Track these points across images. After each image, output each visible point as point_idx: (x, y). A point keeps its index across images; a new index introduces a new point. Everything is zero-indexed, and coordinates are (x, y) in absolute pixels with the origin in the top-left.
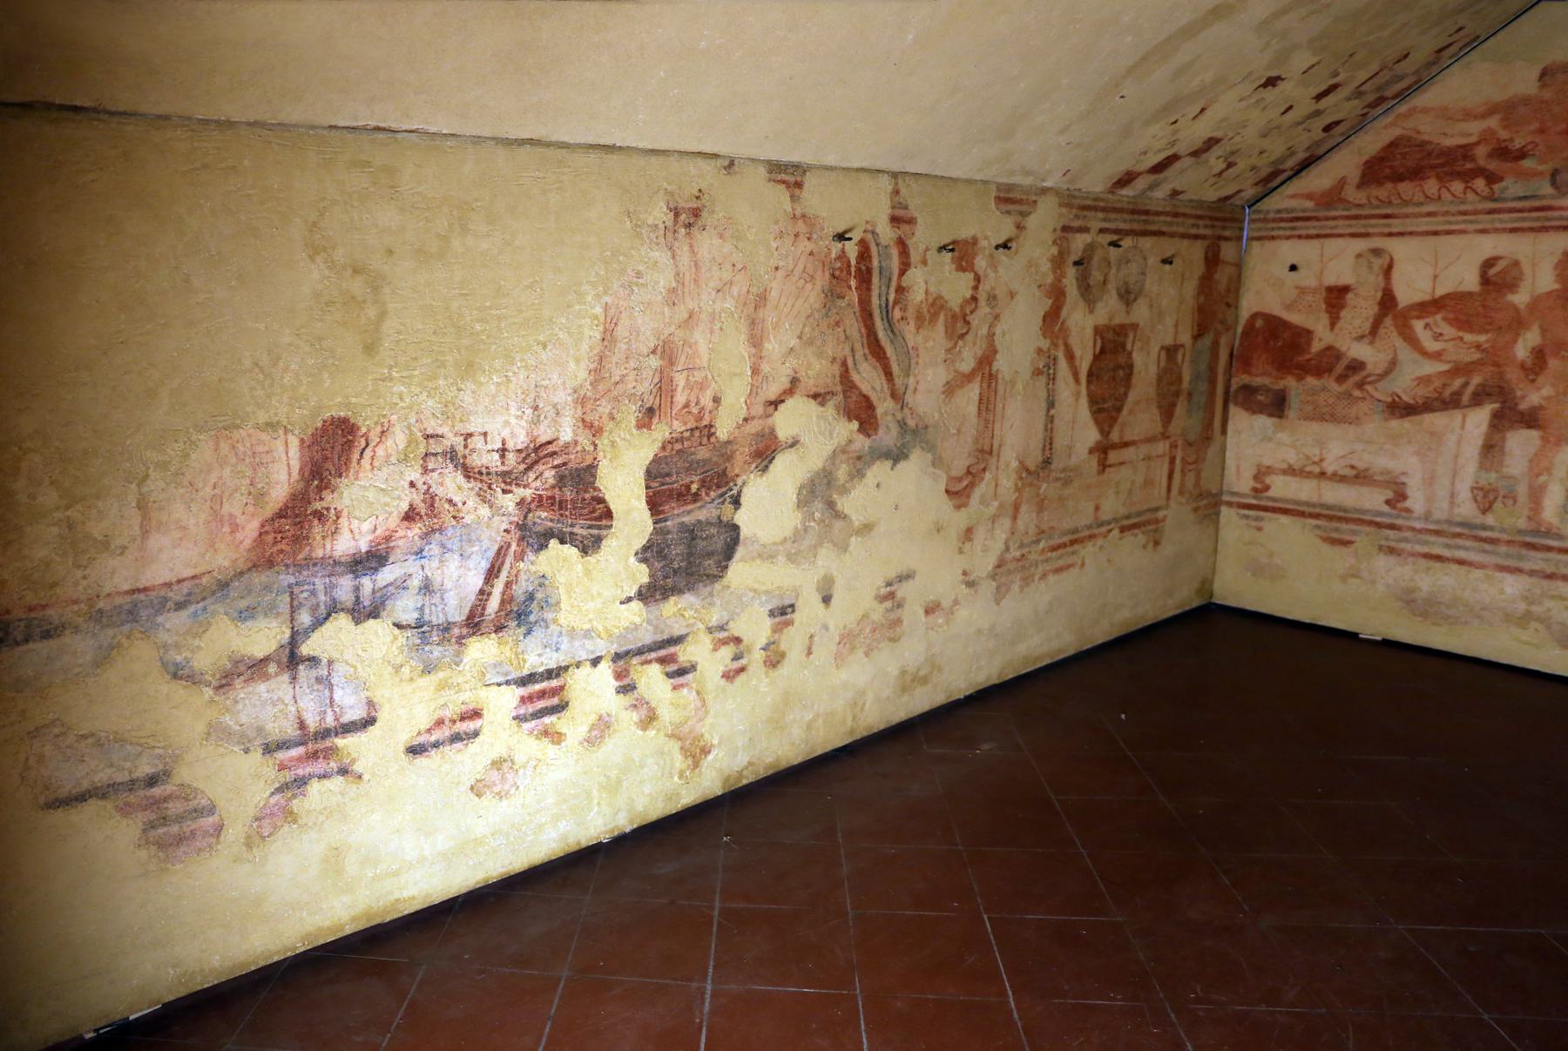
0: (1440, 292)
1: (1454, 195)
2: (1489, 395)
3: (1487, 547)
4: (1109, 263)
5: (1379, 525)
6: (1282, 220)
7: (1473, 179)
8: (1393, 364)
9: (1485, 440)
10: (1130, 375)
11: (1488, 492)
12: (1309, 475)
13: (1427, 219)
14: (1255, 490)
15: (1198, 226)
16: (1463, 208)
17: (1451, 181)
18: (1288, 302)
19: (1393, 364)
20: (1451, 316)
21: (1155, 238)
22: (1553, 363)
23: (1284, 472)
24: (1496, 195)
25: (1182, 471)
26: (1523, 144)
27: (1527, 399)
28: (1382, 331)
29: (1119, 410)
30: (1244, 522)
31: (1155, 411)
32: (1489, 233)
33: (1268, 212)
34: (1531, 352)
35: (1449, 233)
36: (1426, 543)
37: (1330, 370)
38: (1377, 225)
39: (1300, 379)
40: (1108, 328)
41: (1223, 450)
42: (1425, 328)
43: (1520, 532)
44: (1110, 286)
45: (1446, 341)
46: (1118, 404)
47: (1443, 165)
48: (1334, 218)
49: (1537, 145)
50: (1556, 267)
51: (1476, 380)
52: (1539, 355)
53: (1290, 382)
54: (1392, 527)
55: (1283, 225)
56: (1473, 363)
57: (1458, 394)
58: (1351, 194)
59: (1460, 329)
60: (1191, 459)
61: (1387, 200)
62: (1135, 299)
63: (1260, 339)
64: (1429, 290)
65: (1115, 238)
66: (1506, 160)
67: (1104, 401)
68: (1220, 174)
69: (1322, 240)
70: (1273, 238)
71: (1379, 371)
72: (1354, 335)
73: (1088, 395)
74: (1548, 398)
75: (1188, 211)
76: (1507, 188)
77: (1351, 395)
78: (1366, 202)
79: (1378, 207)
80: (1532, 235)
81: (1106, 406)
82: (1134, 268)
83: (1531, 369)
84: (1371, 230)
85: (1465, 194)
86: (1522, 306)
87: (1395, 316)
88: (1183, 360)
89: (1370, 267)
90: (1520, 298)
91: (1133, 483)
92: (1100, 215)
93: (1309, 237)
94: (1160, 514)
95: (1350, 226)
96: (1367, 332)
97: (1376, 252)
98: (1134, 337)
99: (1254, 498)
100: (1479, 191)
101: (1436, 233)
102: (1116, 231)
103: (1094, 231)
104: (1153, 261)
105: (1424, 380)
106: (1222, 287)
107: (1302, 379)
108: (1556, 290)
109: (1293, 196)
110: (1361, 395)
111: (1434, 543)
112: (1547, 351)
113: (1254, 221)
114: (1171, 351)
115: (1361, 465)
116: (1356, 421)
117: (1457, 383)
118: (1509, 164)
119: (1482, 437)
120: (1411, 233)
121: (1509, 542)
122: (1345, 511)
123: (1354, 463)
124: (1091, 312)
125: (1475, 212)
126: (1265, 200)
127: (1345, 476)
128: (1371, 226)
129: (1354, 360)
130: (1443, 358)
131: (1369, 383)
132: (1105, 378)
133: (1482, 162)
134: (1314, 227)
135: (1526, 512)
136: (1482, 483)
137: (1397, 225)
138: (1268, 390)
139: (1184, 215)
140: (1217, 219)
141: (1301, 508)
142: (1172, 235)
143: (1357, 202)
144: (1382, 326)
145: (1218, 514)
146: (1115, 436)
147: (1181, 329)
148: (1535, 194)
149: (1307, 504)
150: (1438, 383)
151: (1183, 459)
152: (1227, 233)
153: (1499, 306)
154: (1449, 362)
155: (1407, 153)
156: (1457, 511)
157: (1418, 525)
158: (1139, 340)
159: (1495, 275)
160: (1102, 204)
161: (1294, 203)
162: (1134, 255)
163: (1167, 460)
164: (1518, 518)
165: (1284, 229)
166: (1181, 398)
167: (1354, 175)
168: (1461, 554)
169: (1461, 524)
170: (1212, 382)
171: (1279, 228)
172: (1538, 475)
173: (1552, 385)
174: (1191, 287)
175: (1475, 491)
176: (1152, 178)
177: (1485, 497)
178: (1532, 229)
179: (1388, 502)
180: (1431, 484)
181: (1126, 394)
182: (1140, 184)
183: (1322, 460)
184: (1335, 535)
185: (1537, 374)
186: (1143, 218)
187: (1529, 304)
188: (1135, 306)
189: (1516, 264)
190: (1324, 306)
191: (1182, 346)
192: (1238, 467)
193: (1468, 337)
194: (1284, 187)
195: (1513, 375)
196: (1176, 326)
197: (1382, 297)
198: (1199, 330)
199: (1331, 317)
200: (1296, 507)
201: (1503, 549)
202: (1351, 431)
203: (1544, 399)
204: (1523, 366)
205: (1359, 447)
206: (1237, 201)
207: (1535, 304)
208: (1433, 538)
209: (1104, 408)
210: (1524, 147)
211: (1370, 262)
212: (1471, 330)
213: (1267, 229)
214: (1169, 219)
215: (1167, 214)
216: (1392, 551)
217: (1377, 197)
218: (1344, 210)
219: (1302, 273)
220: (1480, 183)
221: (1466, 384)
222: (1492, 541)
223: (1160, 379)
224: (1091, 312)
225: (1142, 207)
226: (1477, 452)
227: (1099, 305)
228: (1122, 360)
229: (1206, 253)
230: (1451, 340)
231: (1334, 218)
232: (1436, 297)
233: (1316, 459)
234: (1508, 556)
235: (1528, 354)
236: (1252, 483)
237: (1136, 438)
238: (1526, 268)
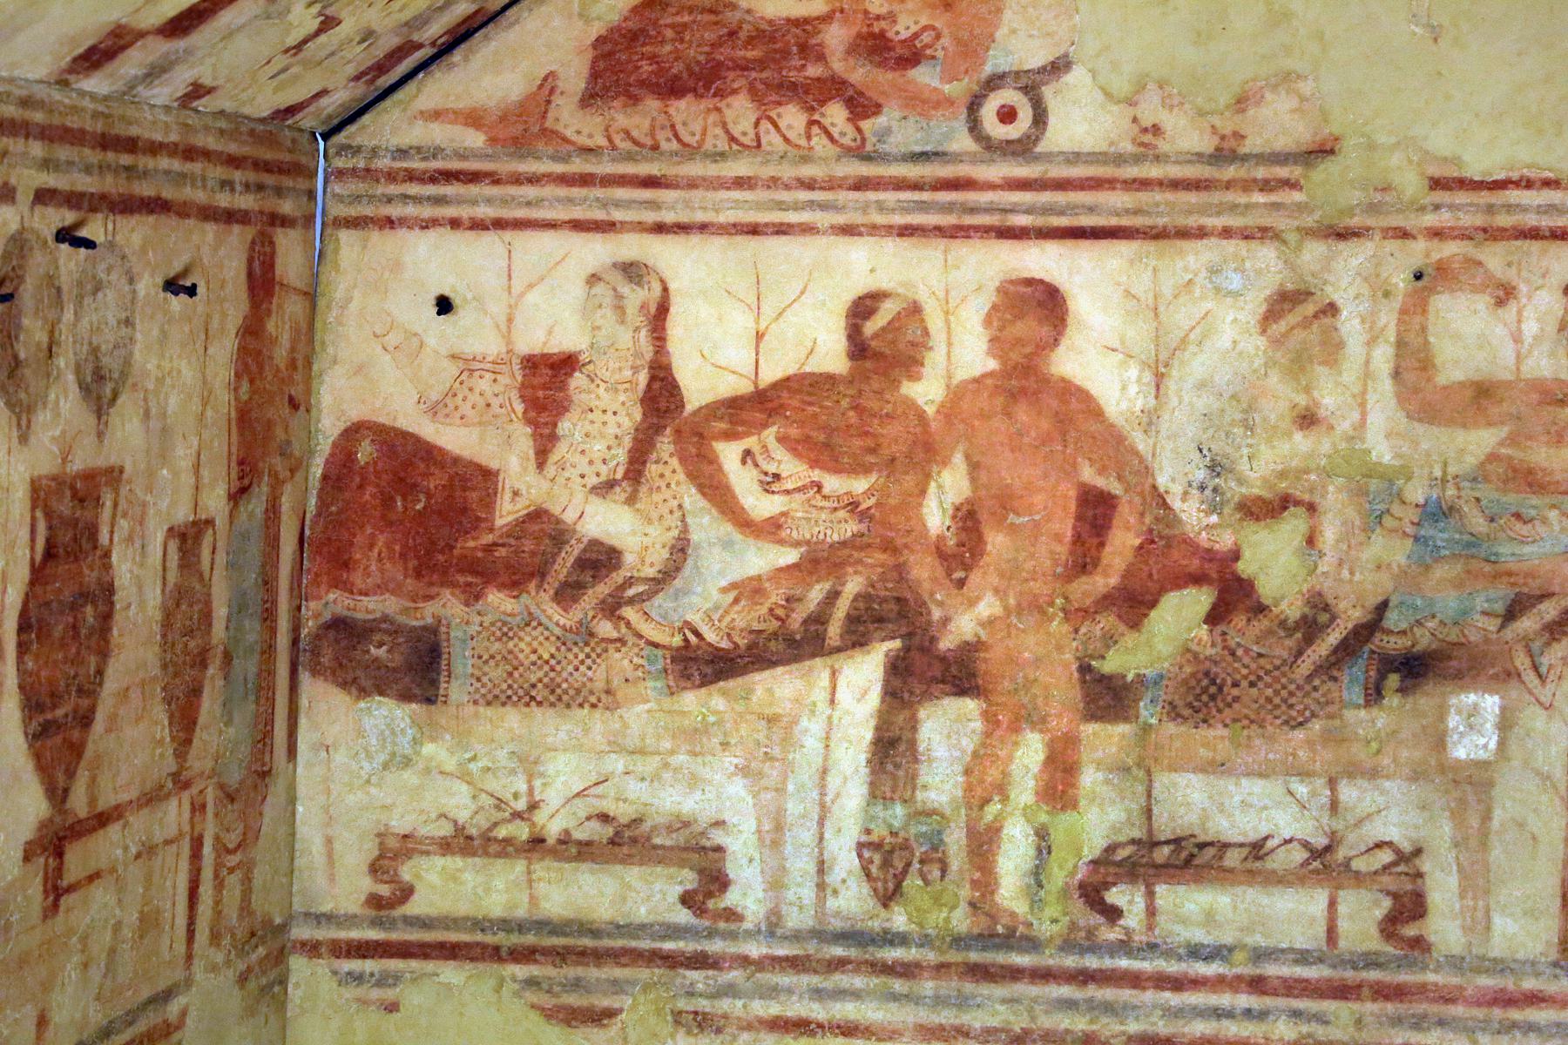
0: (771, 373)
1: (786, 140)
2: (880, 620)
3: (898, 985)
4: (59, 290)
5: (672, 961)
6: (411, 176)
7: (823, 103)
8: (681, 549)
9: (878, 729)
10: (107, 617)
11: (891, 852)
12: (506, 849)
13: (736, 194)
14: (375, 901)
15: (226, 184)
16: (807, 171)
17: (780, 104)
18: (434, 396)
19: (681, 549)
20: (794, 432)
21: (151, 219)
22: (996, 542)
23: (445, 847)
24: (869, 147)
25: (216, 876)
26: (914, 29)
27: (952, 626)
28: (652, 469)
29: (85, 720)
30: (351, 992)
31: (160, 713)
32: (860, 234)
33: (374, 152)
34: (954, 517)
35: (782, 230)
36: (772, 992)
37: (541, 573)
38: (627, 204)
39: (473, 596)
40: (60, 482)
41: (292, 800)
42: (744, 462)
43: (959, 941)
44: (61, 362)
45: (788, 492)
46: (85, 703)
47: (761, 64)
48: (533, 180)
49: (938, 37)
50: (987, 322)
51: (853, 586)
52: (968, 519)
53: (448, 607)
54: (701, 961)
55: (414, 189)
56: (843, 544)
57: (819, 619)
58: (569, 119)
59: (814, 464)
60: (232, 839)
61: (649, 142)
62: (115, 396)
63: (368, 495)
64: (749, 369)
65: (69, 217)
66: (882, 64)
67: (56, 698)
68: (299, 47)
69: (508, 235)
70: (390, 223)
71: (650, 572)
72: (593, 481)
73: (21, 687)
74: (989, 623)
75: (211, 142)
76: (888, 131)
77: (592, 635)
78: (602, 141)
79: (630, 157)
80: (942, 243)
81: (60, 712)
82: (108, 307)
83: (954, 556)
84: (618, 215)
85: (809, 138)
86: (930, 410)
87: (678, 432)
88: (111, 540)
89: (620, 309)
90: (926, 391)
91: (117, 927)
92: (37, 149)
93: (478, 225)
94: (174, 1008)
95: (570, 200)
96: (619, 476)
97: (632, 271)
98: (116, 505)
99: (376, 923)
100: (835, 132)
101: (754, 230)
102: (72, 199)
103: (24, 197)
104: (149, 285)
105: (749, 590)
106: (281, 354)
107: (477, 597)
108: (991, 374)
109: (436, 115)
110: (615, 635)
111: (790, 991)
112: (983, 516)
113: (340, 173)
114: (188, 537)
115: (623, 812)
116: (605, 699)
117: (816, 594)
118: (890, 75)
119: (873, 723)
120: (703, 227)
121: (941, 968)
122: (595, 933)
123: (609, 807)
124: (24, 439)
125: (832, 185)
126: (366, 119)
127: (588, 844)
128: (618, 204)
129: (595, 544)
130: (784, 534)
131: (631, 601)
132: (58, 631)
133: (838, 66)
134: (489, 201)
135: (965, 892)
136: (879, 832)
137: (673, 206)
138: (396, 630)
139: (206, 154)
140: (267, 167)
141: (489, 939)
142: (181, 210)
143: (583, 140)
144: (654, 456)
145: (283, 981)
146: (79, 803)
147: (205, 473)
148: (940, 149)
149: (505, 925)
150: (776, 597)
151: (217, 838)
152: (287, 207)
153: (888, 408)
154: (797, 544)
155: (685, 25)
156: (832, 904)
157: (755, 950)
158: (125, 515)
159: (876, 336)
160: (38, 117)
161: (439, 134)
162: (109, 270)
163: (186, 848)
164: (953, 908)
165: (417, 200)
166: (211, 671)
167: (574, 78)
168: (847, 1010)
169: (843, 937)
170: (268, 616)
171: (405, 197)
172: (987, 801)
173: (996, 591)
174: (224, 349)
175: (867, 854)
176: (159, 48)
177: (886, 864)
178: (940, 231)
179: (687, 900)
180: (776, 844)
181: (100, 672)
182: (131, 64)
183: (533, 806)
184: (572, 1000)
185: (968, 568)
186: (126, 159)
187: (942, 405)
188: (114, 416)
189: (915, 310)
190: (519, 408)
191: (210, 522)
192: (329, 841)
193: (834, 484)
194: (411, 87)
195: (923, 570)
196: (197, 468)
197: (649, 386)
198: (241, 478)
199: (536, 436)
200: (478, 937)
201: (928, 986)
202: (598, 724)
203: (982, 624)
204: (941, 553)
205: (617, 764)
206: (307, 120)
207: (953, 405)
208: (785, 979)
209: (55, 721)
210: (916, 35)
211: (619, 297)
212: (837, 469)
213: (371, 198)
214: (176, 165)
215: (172, 150)
216: (703, 1022)
217: (627, 133)
218: (555, 158)
219: (463, 317)
220: (836, 114)
221: (833, 596)
222: (906, 971)
223: (167, 623)
224: (24, 439)
225: (120, 130)
226: (863, 758)
227: (42, 417)
228: (91, 576)
229: (250, 261)
230: (798, 490)
231: (533, 180)
232: (762, 385)
233: (521, 805)
234: (939, 1001)
235: (948, 523)
236: (366, 885)
237: (124, 797)
238: (935, 322)
